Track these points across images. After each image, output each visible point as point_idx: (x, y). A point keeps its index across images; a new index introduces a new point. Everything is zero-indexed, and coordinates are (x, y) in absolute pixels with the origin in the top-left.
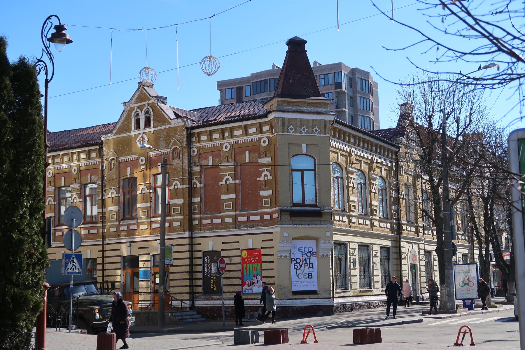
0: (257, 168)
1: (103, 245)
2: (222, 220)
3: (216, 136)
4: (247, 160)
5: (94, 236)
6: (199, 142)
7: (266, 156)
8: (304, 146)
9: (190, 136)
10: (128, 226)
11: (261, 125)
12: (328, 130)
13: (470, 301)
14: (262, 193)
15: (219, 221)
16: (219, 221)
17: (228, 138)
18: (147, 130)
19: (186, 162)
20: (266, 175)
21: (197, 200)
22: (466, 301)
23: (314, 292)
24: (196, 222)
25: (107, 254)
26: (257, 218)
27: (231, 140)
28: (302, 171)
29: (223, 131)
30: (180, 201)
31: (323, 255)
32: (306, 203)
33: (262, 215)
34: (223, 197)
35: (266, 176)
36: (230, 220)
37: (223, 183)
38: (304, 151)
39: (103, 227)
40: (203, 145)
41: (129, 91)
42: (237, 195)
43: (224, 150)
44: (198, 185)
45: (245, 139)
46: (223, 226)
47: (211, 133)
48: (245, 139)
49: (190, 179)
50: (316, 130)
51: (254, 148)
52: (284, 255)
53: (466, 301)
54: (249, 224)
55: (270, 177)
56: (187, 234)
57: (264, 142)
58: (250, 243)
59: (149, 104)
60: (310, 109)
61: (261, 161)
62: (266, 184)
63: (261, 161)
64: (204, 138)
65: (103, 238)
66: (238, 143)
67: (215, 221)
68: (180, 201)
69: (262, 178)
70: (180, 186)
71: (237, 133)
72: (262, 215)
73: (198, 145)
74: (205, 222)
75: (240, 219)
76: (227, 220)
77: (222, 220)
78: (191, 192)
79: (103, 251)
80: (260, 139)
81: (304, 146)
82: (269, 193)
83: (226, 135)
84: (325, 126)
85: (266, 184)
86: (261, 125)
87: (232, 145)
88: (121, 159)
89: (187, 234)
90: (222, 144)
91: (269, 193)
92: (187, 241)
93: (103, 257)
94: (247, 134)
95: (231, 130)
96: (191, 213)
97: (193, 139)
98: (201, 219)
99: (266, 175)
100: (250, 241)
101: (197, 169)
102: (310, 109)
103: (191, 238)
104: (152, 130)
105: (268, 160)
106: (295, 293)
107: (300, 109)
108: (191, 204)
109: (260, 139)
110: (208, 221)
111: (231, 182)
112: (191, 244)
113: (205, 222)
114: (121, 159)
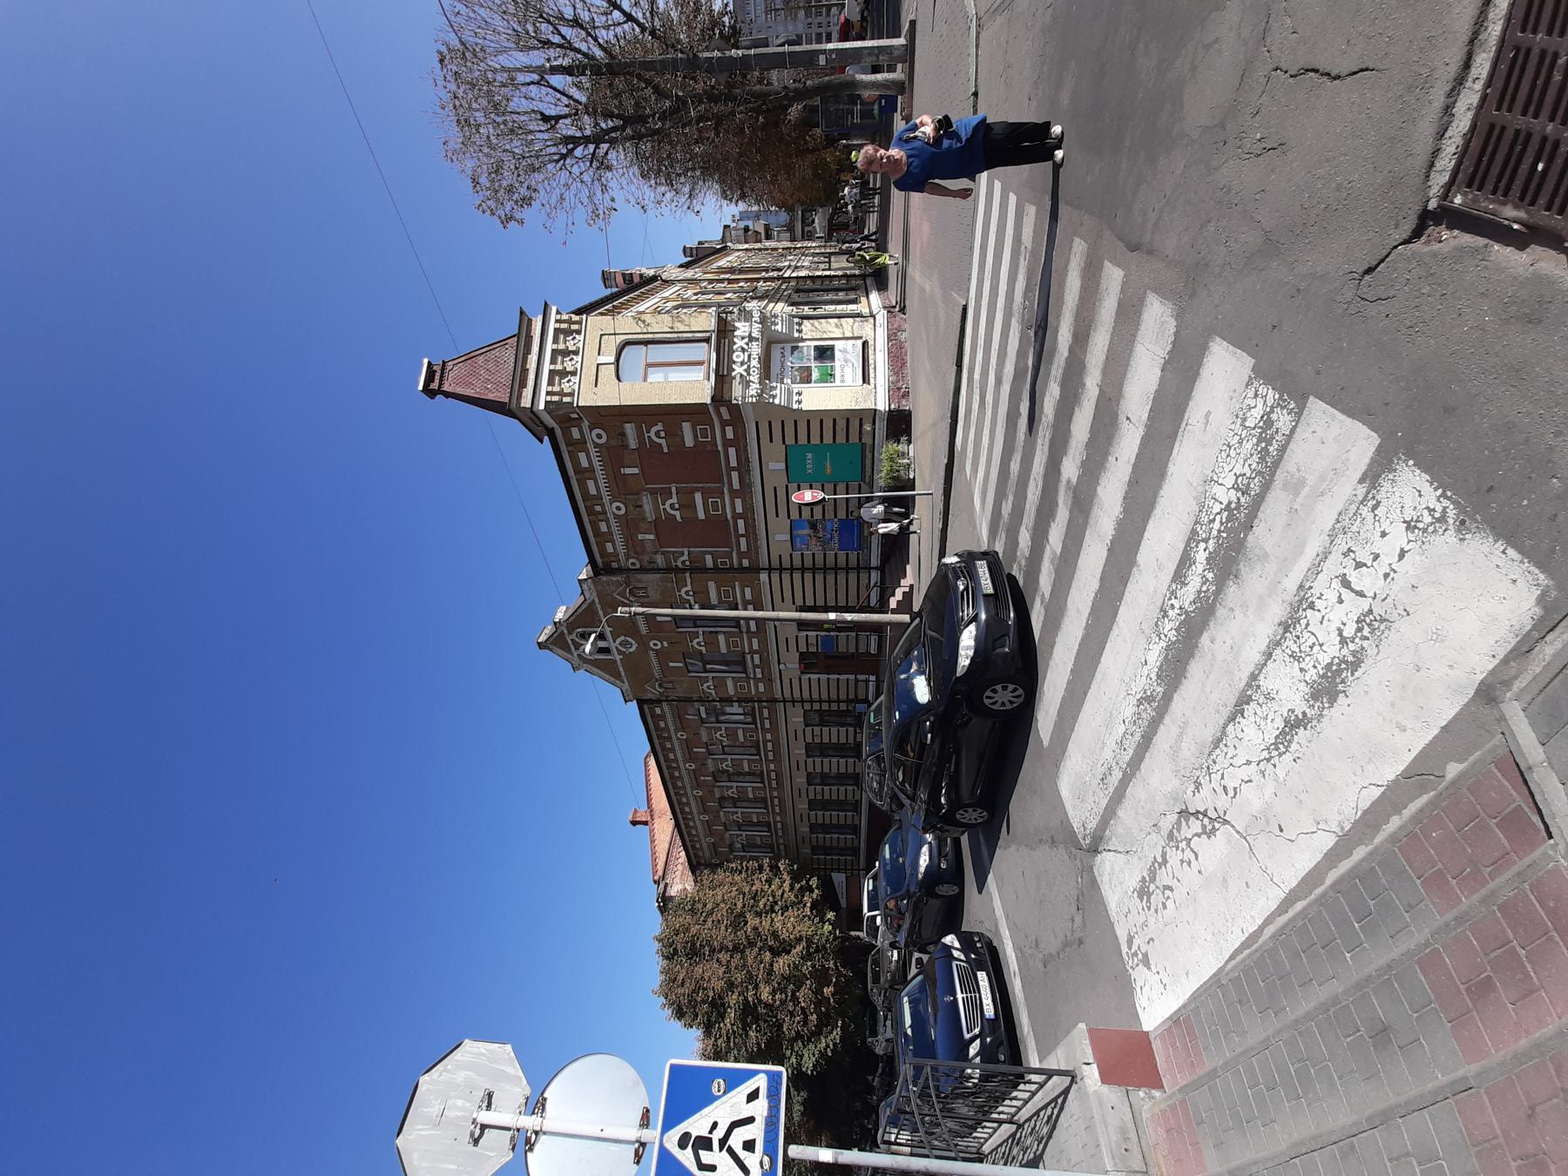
0: (647, 453)
1: (784, 701)
2: (740, 516)
4: (636, 471)
5: (773, 713)
7: (623, 434)
8: (602, 359)
9: (609, 570)
10: (755, 667)
11: (570, 442)
14: (689, 442)
15: (741, 523)
16: (741, 523)
17: (603, 505)
18: (609, 635)
19: (650, 576)
20: (656, 434)
23: (865, 344)
24: (746, 563)
25: (797, 695)
26: (732, 451)
27: (606, 499)
29: (591, 512)
30: (712, 586)
33: (727, 443)
34: (701, 515)
35: (657, 434)
36: (738, 502)
37: (677, 514)
38: (612, 359)
39: (759, 701)
40: (621, 550)
41: (555, 662)
42: (697, 489)
43: (623, 512)
44: (685, 557)
45: (600, 474)
46: (748, 515)
48: (600, 474)
49: (677, 570)
51: (614, 454)
54: (743, 466)
55: (659, 427)
56: (764, 576)
57: (599, 437)
59: (570, 633)
61: (633, 444)
62: (673, 434)
63: (633, 444)
65: (776, 701)
67: (742, 531)
68: (712, 586)
69: (663, 441)
70: (689, 588)
72: (727, 443)
73: (622, 557)
75: (736, 486)
76: (739, 510)
77: (740, 516)
78: (697, 569)
79: (793, 702)
80: (596, 445)
82: (686, 427)
83: (598, 508)
85: (673, 434)
88: (657, 673)
89: (764, 576)
90: (616, 516)
91: (686, 427)
93: (802, 701)
94: (591, 470)
96: (732, 569)
97: (614, 565)
98: (741, 555)
99: (656, 434)
100: (772, 466)
103: (770, 570)
105: (630, 429)
106: (865, 380)
108: (716, 569)
109: (596, 445)
110: (743, 541)
111: (674, 500)
112: (781, 569)
113: (744, 547)
114: (657, 673)
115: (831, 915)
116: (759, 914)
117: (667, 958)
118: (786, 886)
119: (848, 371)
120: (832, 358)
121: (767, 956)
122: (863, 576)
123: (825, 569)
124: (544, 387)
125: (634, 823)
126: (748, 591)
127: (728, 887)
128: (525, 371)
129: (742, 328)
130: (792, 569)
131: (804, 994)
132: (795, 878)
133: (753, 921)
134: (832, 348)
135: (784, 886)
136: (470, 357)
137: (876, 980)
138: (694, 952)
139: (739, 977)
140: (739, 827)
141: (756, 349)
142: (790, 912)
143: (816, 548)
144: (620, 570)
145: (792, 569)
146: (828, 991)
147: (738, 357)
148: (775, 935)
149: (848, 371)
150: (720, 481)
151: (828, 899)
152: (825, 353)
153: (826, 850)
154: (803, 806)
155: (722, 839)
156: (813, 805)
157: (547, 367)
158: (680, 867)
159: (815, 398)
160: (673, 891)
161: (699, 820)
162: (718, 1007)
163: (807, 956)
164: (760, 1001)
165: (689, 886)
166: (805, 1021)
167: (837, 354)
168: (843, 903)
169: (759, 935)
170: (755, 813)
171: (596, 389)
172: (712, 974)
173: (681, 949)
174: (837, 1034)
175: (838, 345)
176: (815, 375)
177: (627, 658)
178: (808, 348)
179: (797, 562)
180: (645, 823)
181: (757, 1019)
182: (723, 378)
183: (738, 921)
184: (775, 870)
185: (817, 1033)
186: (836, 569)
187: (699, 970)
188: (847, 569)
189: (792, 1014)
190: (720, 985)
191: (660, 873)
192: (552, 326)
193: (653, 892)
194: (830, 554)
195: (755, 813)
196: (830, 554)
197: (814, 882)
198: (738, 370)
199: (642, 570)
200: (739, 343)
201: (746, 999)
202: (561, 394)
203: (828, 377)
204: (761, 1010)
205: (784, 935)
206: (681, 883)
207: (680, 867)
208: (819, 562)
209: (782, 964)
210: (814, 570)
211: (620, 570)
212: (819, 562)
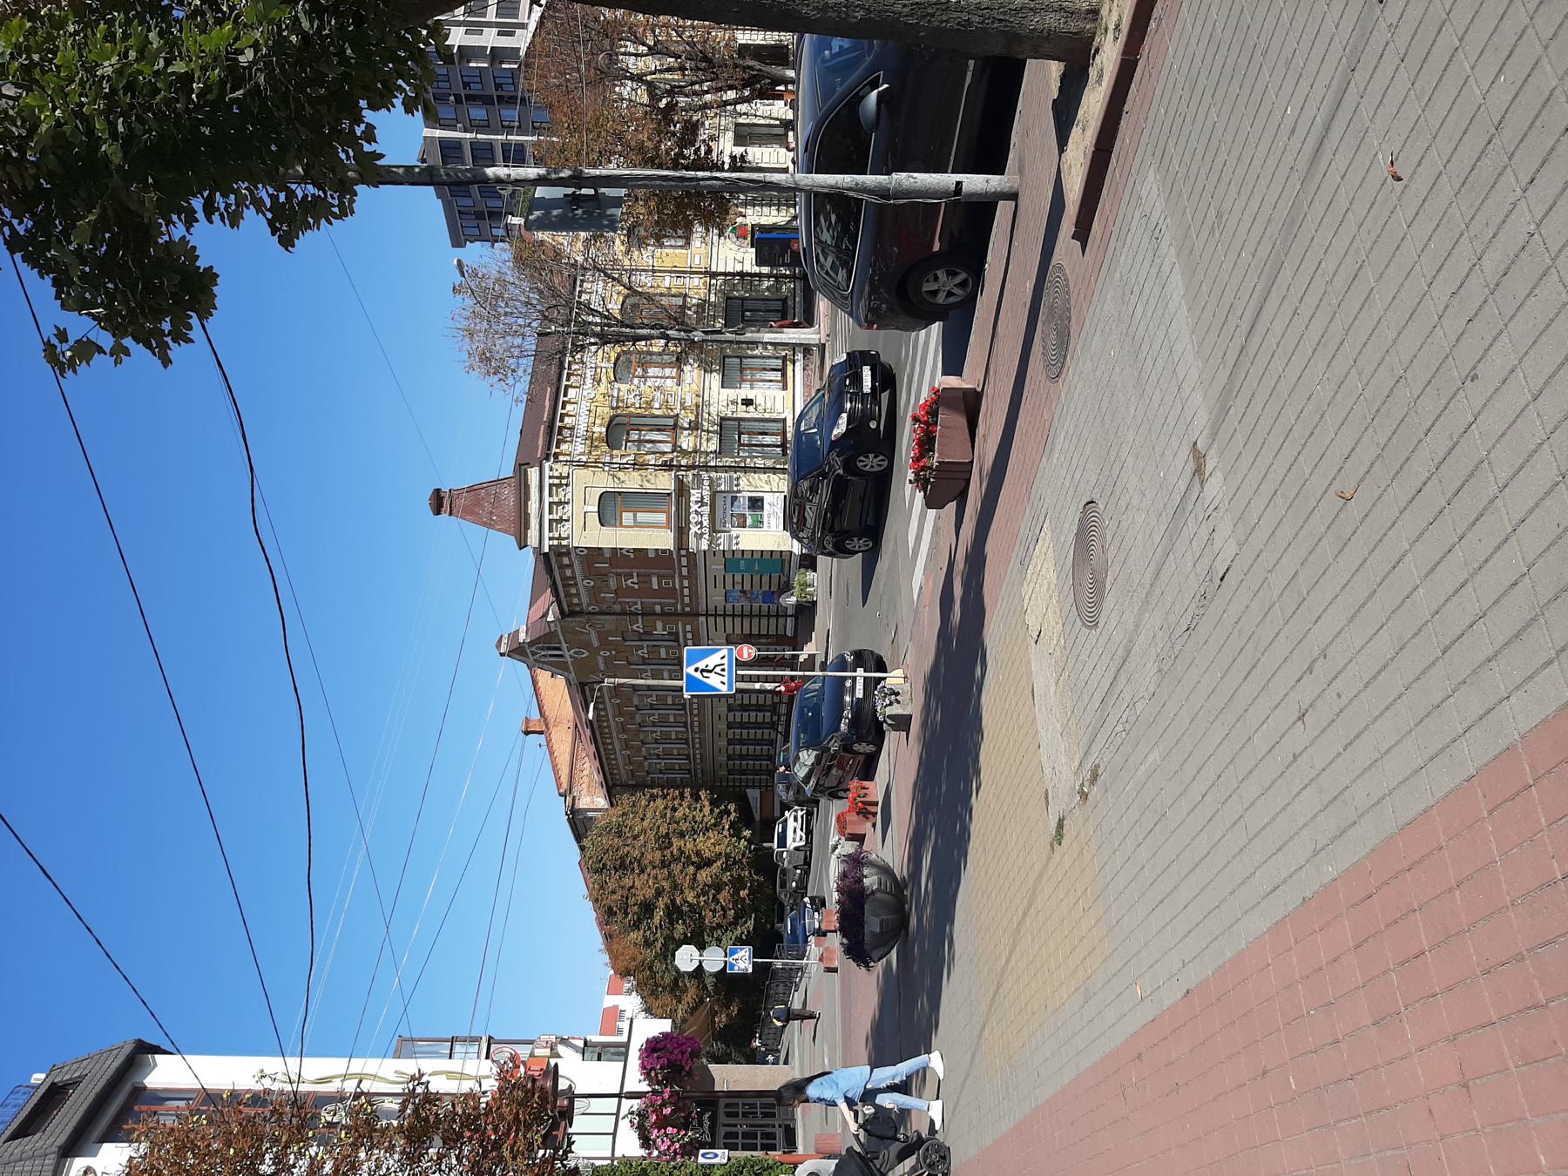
3: (573, 591)
6: (580, 604)
9: (572, 614)
14: (652, 555)
21: (658, 608)
26: (684, 561)
27: (579, 579)
30: (659, 625)
33: (679, 556)
34: (655, 586)
36: (686, 583)
40: (585, 599)
47: (568, 595)
58: (717, 567)
64: (576, 601)
66: (583, 572)
68: (659, 625)
71: (568, 573)
74: (687, 600)
78: (647, 613)
86: (560, 555)
87: (586, 578)
89: (702, 619)
92: (711, 619)
94: (570, 566)
95: (564, 578)
96: (675, 614)
101: (617, 608)
103: (707, 615)
104: (565, 646)
108: (663, 614)
112: (716, 615)
115: (747, 833)
116: (682, 835)
117: (596, 871)
118: (707, 810)
119: (773, 520)
120: (762, 508)
121: (692, 869)
122: (781, 620)
123: (751, 616)
124: (547, 534)
125: (527, 733)
126: (688, 628)
127: (651, 813)
128: (527, 516)
129: (695, 495)
130: (725, 616)
131: (724, 896)
132: (713, 803)
133: (677, 843)
134: (761, 500)
135: (705, 812)
136: (471, 489)
137: (783, 885)
138: (623, 866)
139: (666, 885)
140: (658, 757)
141: (706, 509)
142: (710, 834)
143: (747, 604)
144: (581, 613)
145: (725, 616)
146: (743, 893)
147: (693, 518)
148: (698, 853)
149: (773, 520)
150: (673, 568)
151: (745, 818)
152: (756, 503)
153: (742, 772)
154: (723, 743)
155: (641, 764)
156: (730, 742)
157: (547, 517)
158: (586, 779)
159: (750, 540)
160: (583, 803)
161: (620, 755)
162: (648, 908)
163: (727, 868)
164: (686, 901)
165: (601, 802)
166: (724, 916)
167: (766, 506)
168: (757, 818)
169: (683, 852)
170: (675, 748)
171: (588, 534)
172: (643, 886)
173: (606, 864)
174: (750, 924)
175: (768, 498)
176: (749, 521)
177: (575, 661)
178: (743, 502)
179: (729, 610)
180: (541, 733)
181: (681, 914)
182: (681, 533)
183: (664, 842)
184: (697, 799)
185: (735, 924)
186: (760, 616)
187: (627, 882)
188: (769, 616)
189: (714, 911)
190: (650, 893)
191: (565, 786)
192: (547, 482)
193: (560, 807)
194: (756, 606)
195: (675, 748)
196: (756, 606)
197: (732, 807)
198: (694, 529)
199: (601, 613)
200: (694, 507)
201: (673, 901)
202: (560, 538)
203: (758, 523)
204: (685, 909)
205: (707, 854)
206: (593, 799)
207: (586, 779)
208: (747, 611)
209: (704, 876)
210: (742, 616)
211: (581, 613)
212: (747, 611)
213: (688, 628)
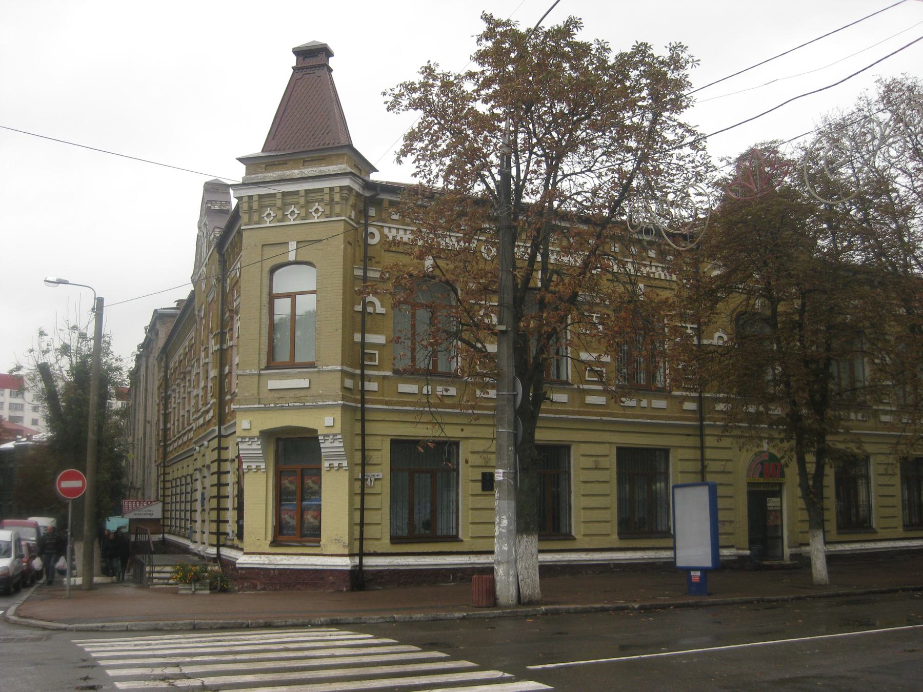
12: (337, 209)
13: (698, 573)
22: (692, 573)
28: (292, 296)
31: (331, 467)
32: (298, 360)
38: (292, 257)
50: (317, 211)
52: (254, 466)
53: (692, 573)
60: (307, 171)
81: (292, 245)
84: (332, 200)
102: (307, 171)
103: (220, 436)
107: (288, 173)
192: (325, 184)
213: (211, 413)
